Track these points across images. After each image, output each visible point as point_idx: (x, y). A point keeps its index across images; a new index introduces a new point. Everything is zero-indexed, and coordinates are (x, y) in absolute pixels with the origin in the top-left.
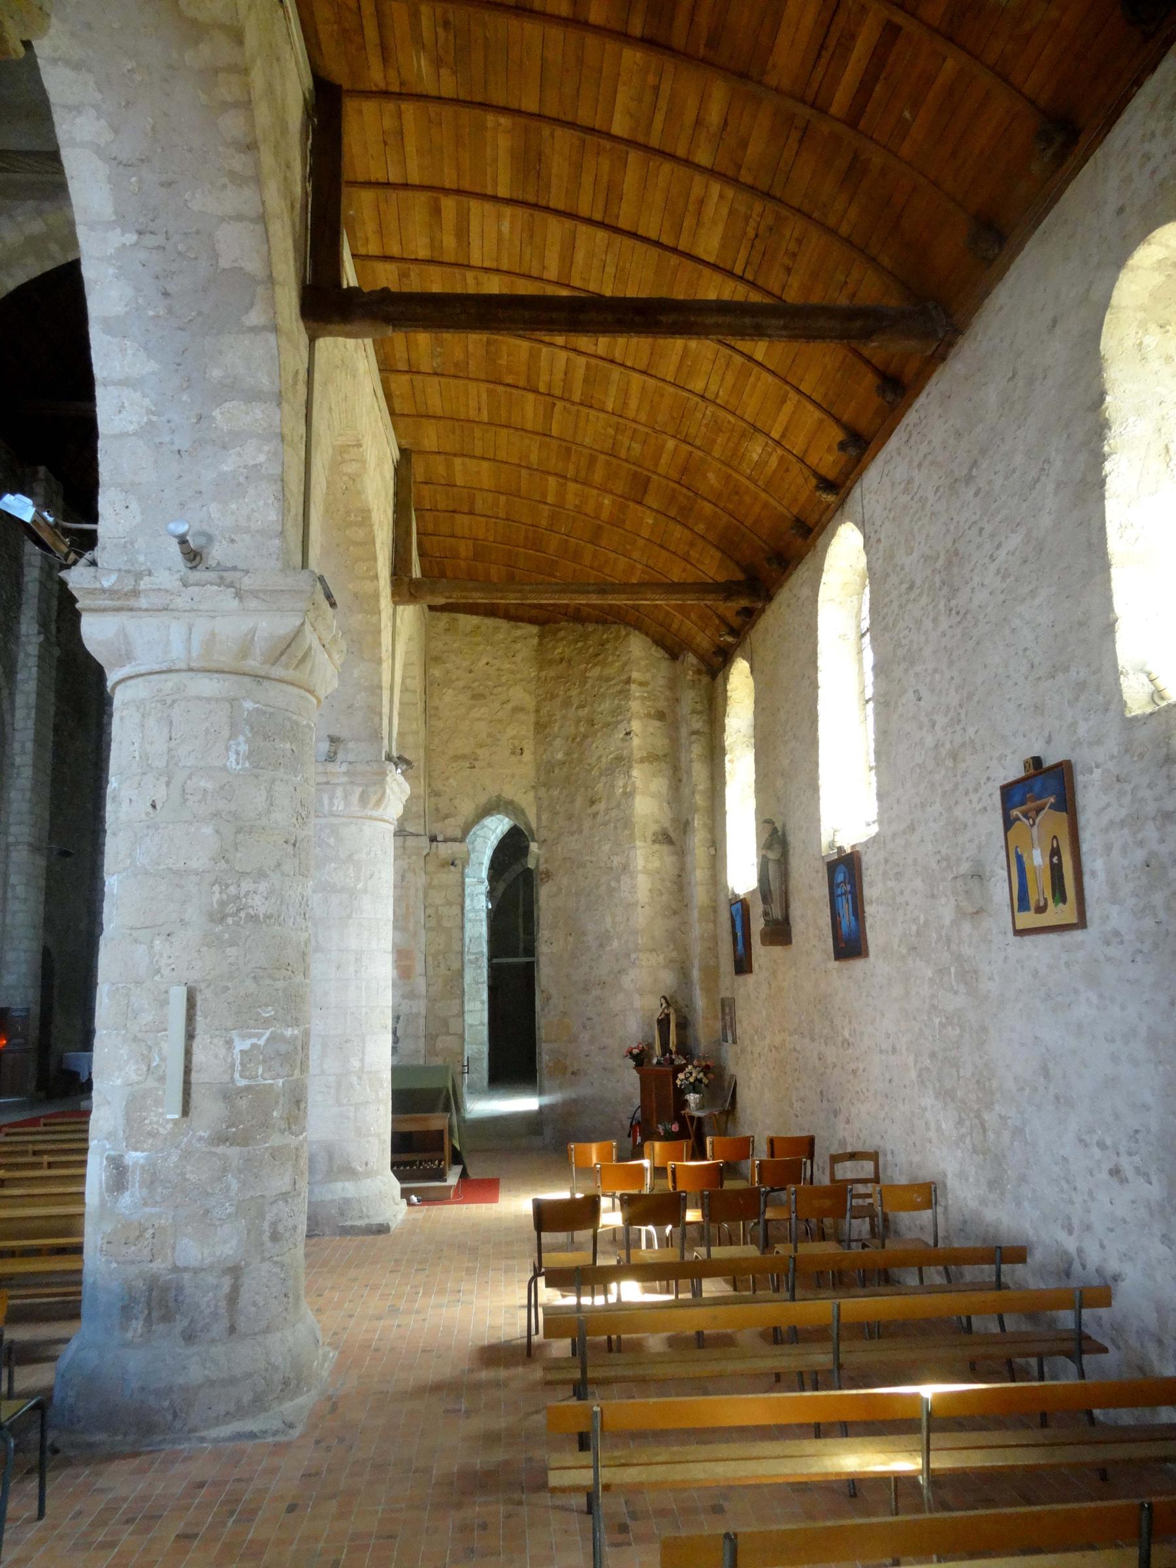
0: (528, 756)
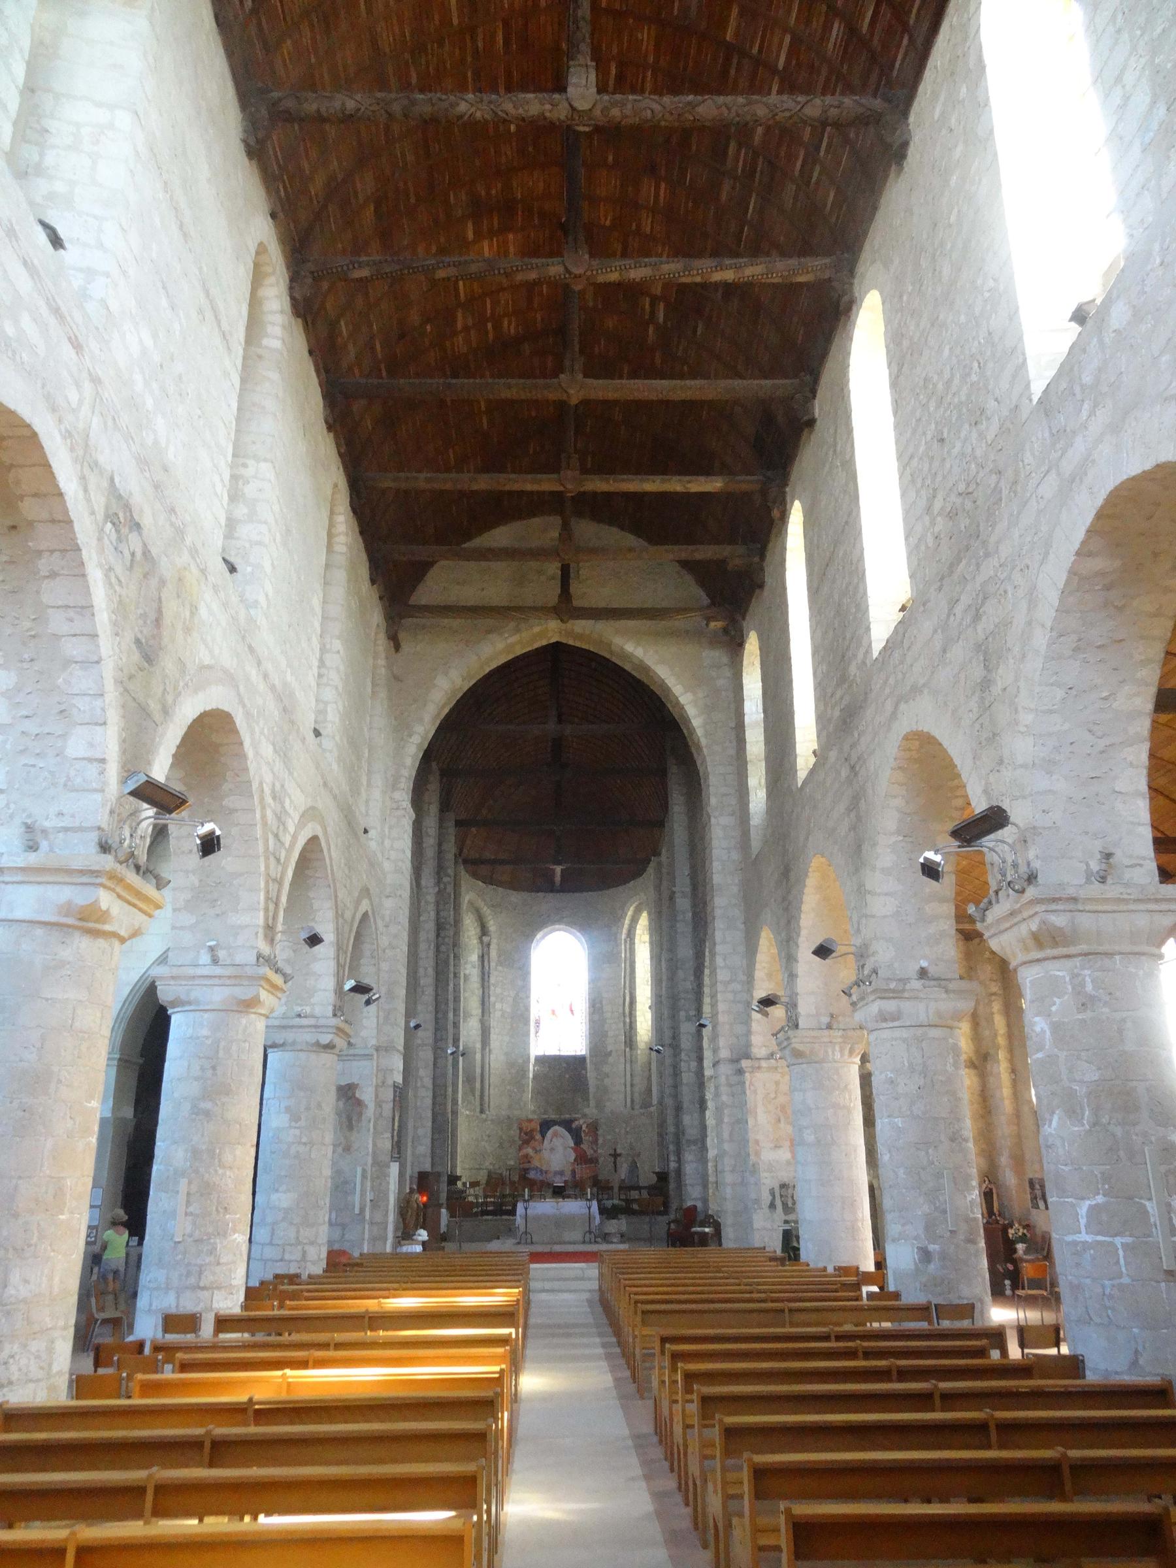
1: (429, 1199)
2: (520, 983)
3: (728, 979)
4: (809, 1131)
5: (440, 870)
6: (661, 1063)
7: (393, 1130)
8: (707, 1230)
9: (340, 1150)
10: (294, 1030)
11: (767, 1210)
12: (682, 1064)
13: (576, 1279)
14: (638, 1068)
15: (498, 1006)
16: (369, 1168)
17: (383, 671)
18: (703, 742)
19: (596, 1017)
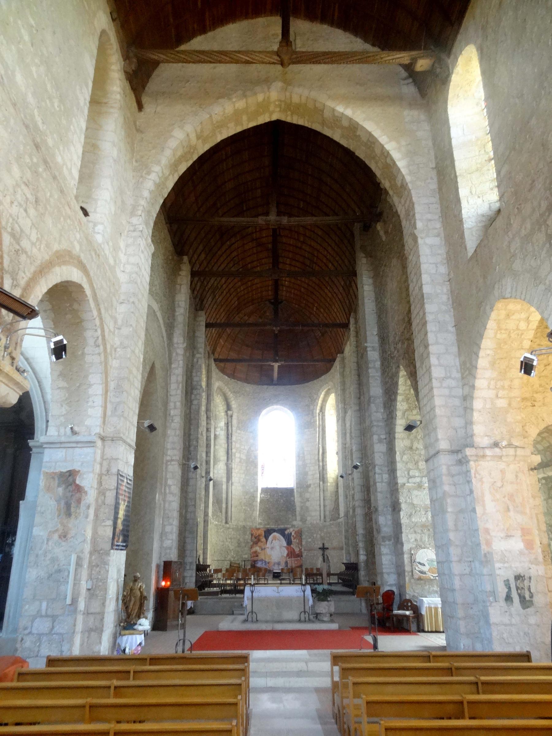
1: (172, 583)
2: (252, 441)
3: (443, 375)
5: (191, 347)
6: (347, 487)
7: (116, 518)
8: (408, 613)
9: (56, 537)
11: (502, 603)
12: (377, 476)
13: (299, 674)
14: (328, 494)
15: (237, 455)
16: (86, 555)
17: (118, 97)
18: (408, 178)
19: (301, 463)
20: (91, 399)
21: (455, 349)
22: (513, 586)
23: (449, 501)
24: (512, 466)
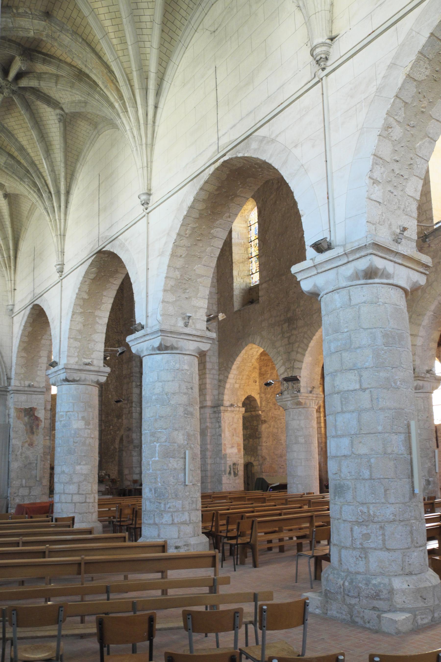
0: (257, 383)
3: (211, 368)
4: (302, 438)
9: (26, 445)
10: (85, 373)
11: (227, 475)
12: (133, 408)
20: (39, 365)
21: (217, 354)
22: (232, 468)
23: (209, 430)
24: (237, 416)
